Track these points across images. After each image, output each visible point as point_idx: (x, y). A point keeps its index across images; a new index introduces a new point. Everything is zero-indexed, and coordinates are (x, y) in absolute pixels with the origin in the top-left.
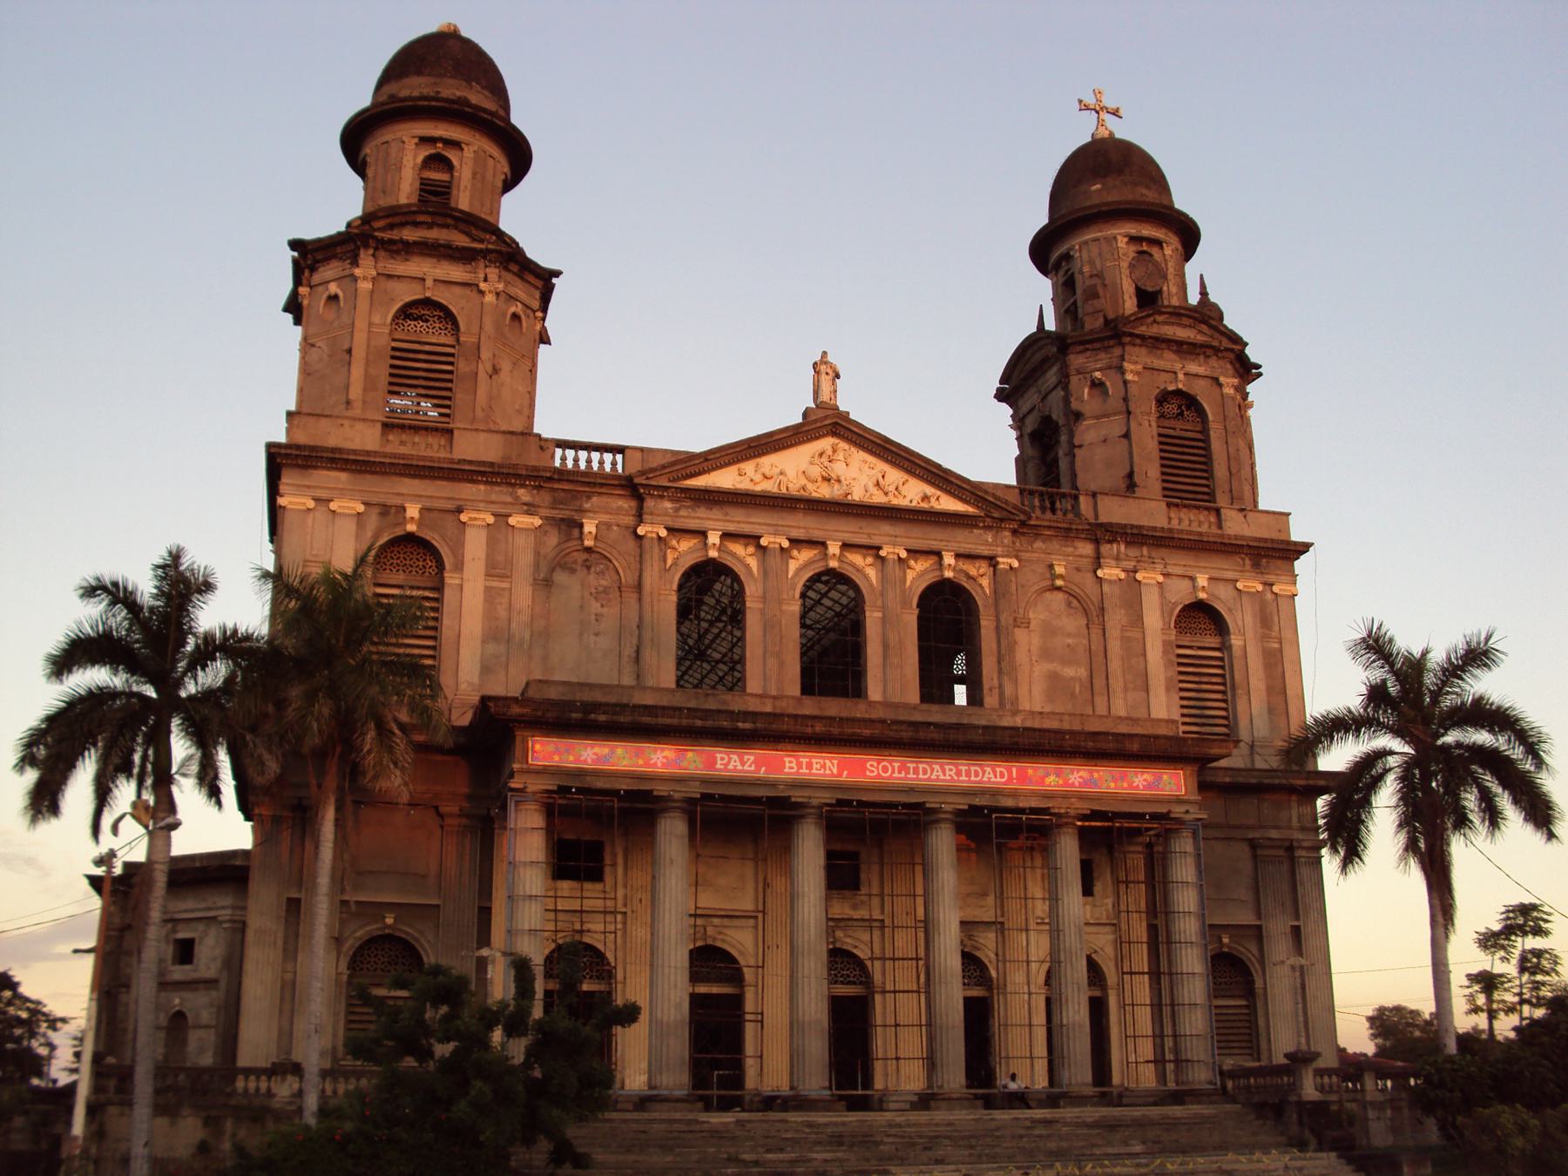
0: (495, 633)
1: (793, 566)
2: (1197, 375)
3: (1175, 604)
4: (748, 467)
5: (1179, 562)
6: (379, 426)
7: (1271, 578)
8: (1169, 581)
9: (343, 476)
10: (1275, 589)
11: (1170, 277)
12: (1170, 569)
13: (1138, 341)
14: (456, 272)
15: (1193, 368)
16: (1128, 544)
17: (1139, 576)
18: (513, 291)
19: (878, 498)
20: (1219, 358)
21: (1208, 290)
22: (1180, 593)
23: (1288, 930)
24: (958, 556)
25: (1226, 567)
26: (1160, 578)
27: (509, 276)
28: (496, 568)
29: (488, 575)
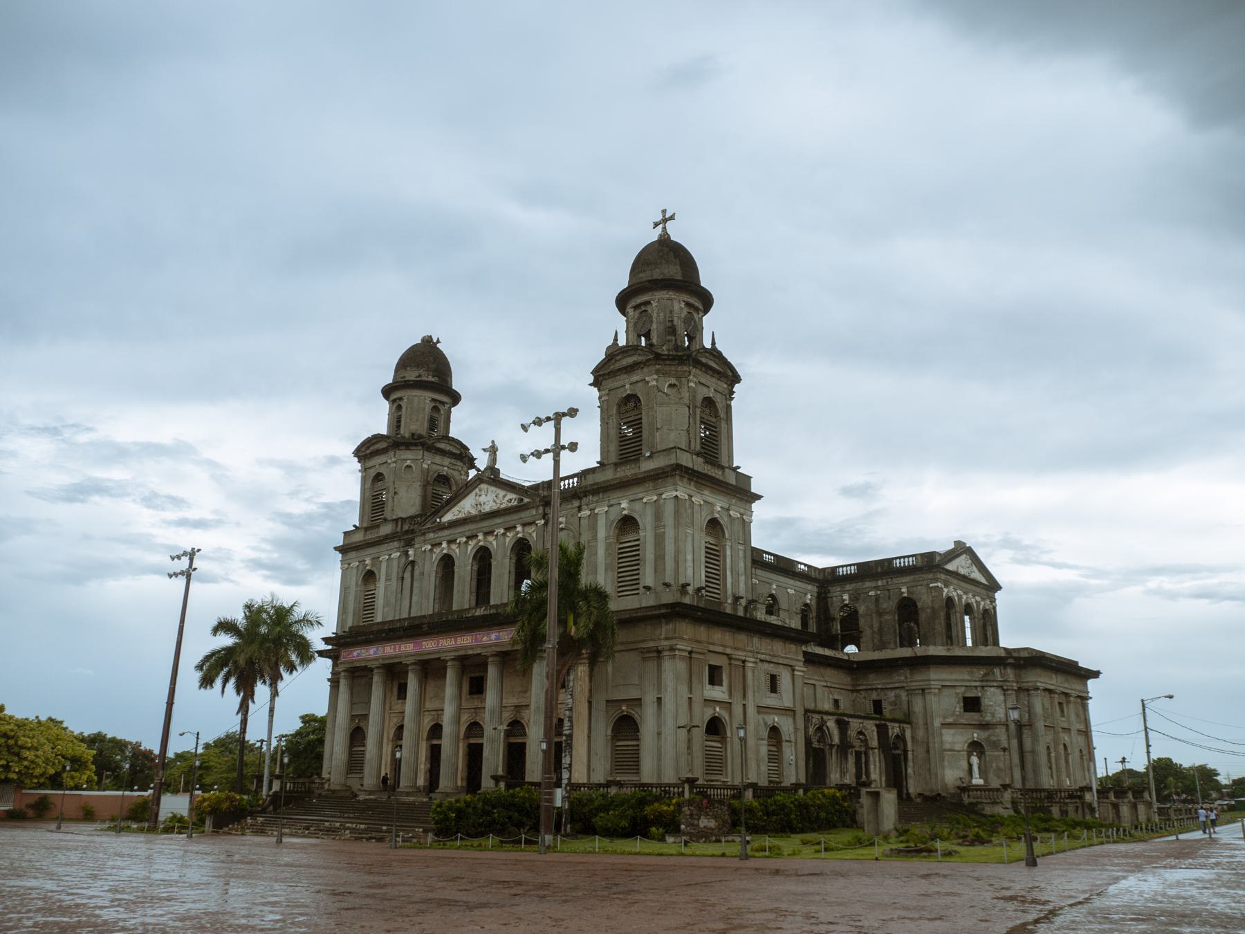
0: (386, 604)
1: (470, 548)
2: (637, 382)
3: (613, 521)
4: (455, 510)
5: (614, 497)
6: (363, 530)
7: (660, 491)
8: (611, 509)
9: (354, 553)
10: (664, 496)
11: (654, 319)
12: (612, 502)
13: (607, 377)
14: (382, 459)
15: (635, 378)
16: (593, 495)
17: (596, 511)
18: (403, 457)
19: (495, 507)
20: (648, 366)
21: (619, 338)
22: (615, 515)
23: (655, 699)
24: (524, 525)
25: (637, 492)
26: (606, 509)
27: (401, 452)
28: (388, 579)
29: (386, 580)
